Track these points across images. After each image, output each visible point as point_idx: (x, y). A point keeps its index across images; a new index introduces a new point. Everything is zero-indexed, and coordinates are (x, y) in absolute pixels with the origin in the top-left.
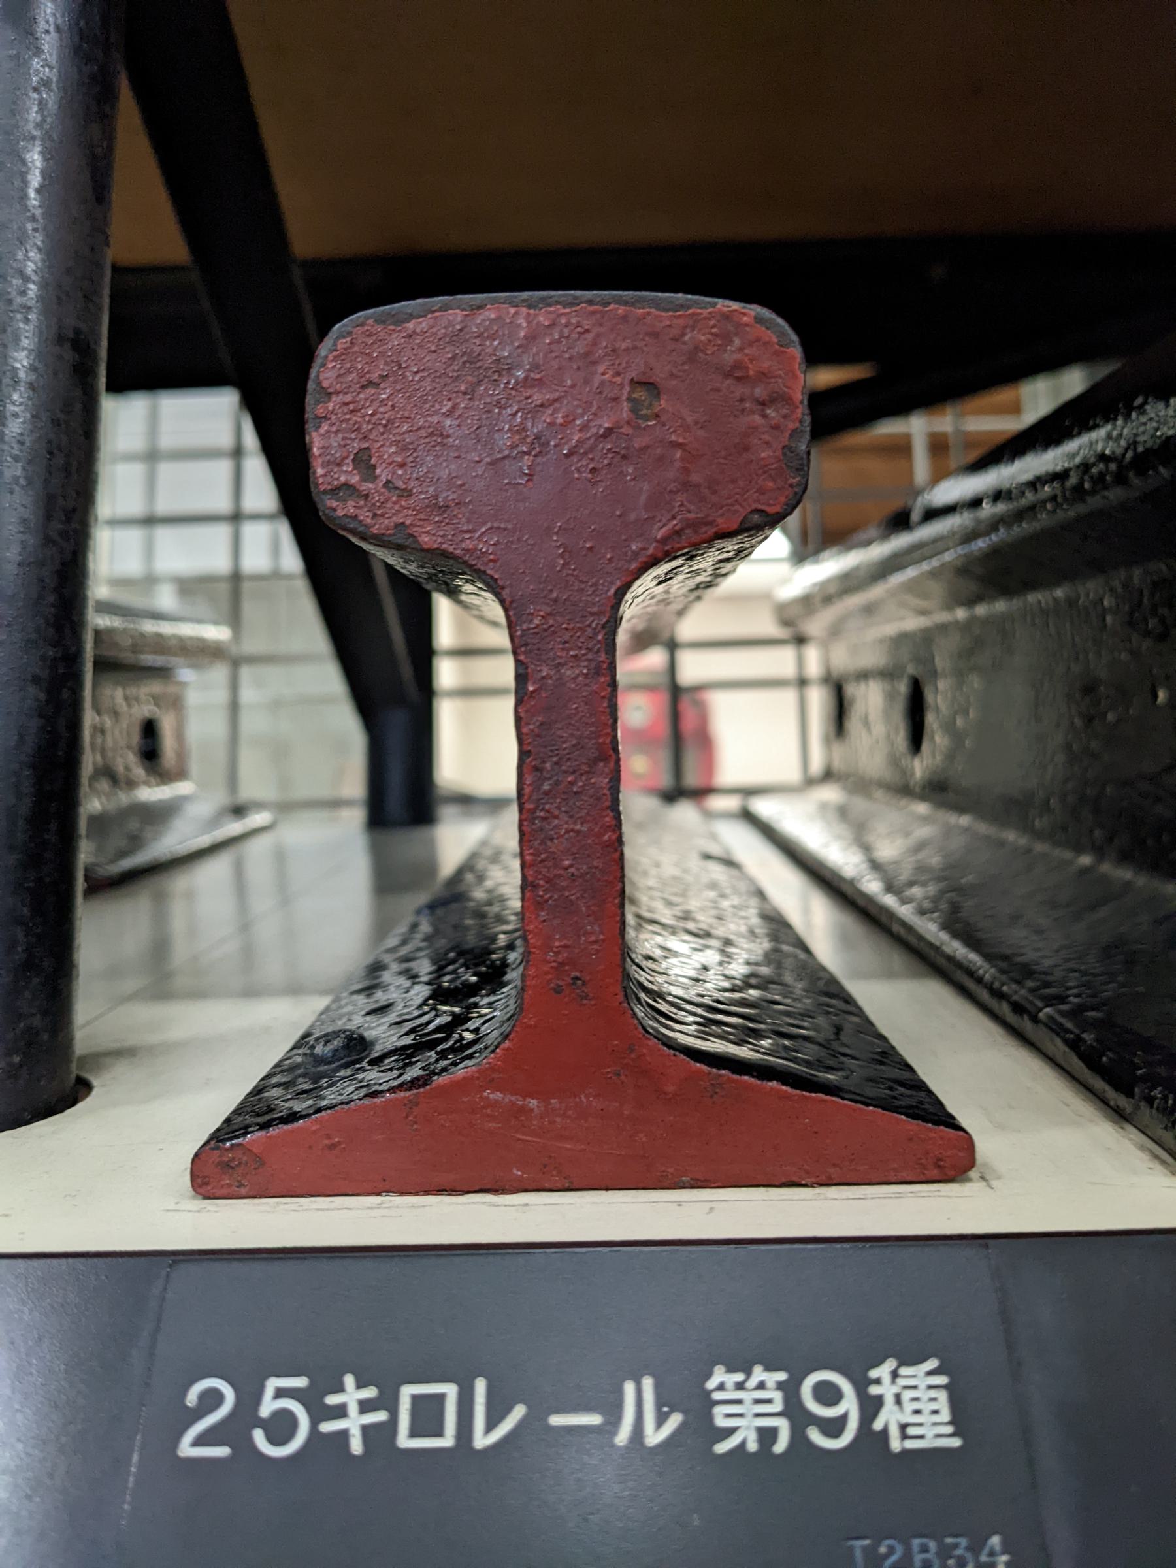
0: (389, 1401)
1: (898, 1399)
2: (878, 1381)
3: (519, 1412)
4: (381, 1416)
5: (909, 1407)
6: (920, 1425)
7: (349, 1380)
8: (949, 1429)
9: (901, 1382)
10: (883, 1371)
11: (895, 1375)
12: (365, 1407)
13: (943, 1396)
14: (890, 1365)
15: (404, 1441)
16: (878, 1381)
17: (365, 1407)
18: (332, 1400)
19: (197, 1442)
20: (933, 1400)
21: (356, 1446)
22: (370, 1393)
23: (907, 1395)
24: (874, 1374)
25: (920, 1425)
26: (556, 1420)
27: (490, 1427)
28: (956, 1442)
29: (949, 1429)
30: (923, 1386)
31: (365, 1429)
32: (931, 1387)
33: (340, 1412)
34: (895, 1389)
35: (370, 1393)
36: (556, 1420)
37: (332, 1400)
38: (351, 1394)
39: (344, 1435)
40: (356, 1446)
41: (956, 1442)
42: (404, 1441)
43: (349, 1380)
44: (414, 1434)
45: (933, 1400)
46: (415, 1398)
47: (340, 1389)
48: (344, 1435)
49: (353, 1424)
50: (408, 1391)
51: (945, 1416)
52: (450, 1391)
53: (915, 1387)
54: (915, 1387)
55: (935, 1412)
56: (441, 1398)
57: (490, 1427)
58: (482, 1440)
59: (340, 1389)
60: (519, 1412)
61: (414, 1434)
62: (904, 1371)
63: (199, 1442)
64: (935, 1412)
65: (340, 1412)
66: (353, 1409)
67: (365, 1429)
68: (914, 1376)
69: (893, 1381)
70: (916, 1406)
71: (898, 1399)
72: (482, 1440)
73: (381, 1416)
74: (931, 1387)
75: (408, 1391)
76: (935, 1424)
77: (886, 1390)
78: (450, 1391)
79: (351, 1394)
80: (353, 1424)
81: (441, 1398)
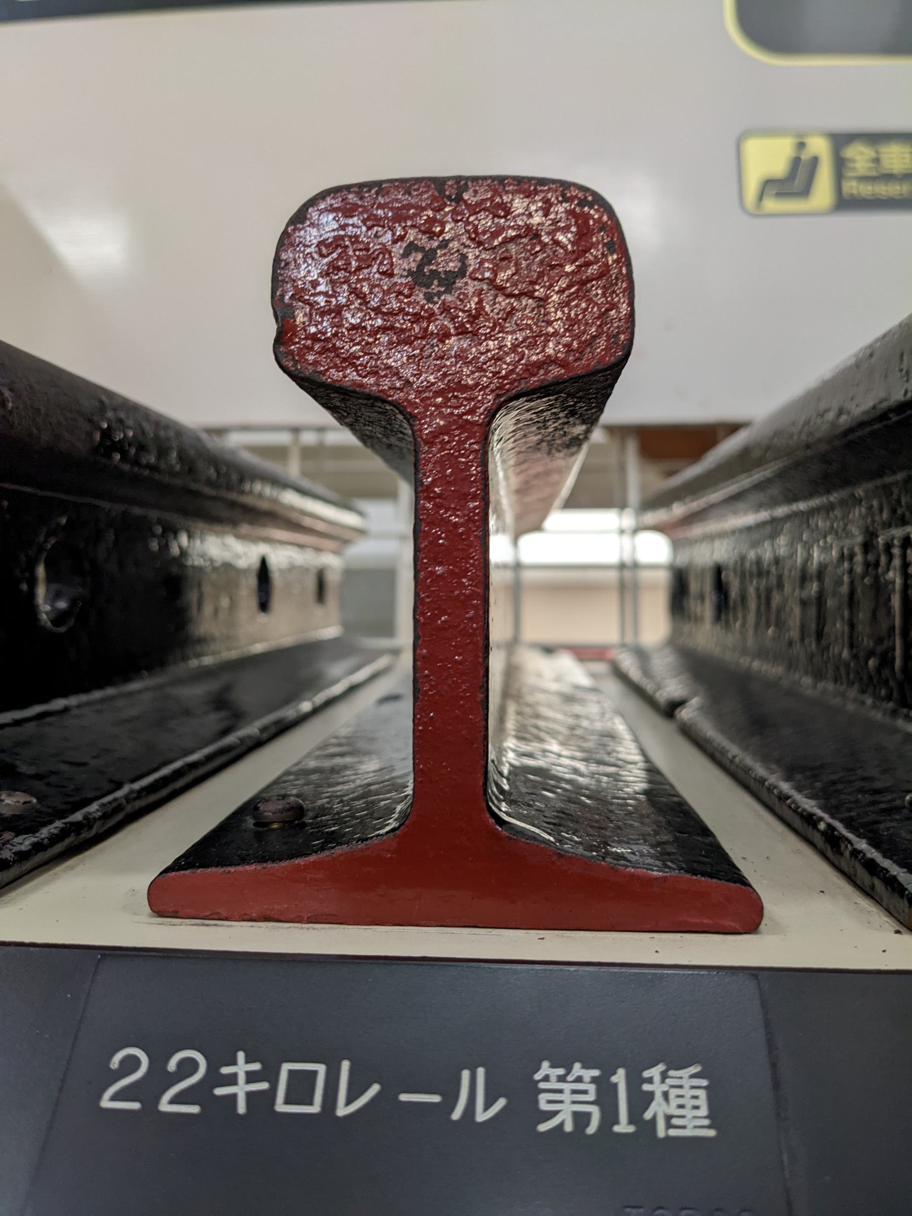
0: (270, 1074)
1: (666, 1095)
2: (650, 1081)
3: (375, 1089)
4: (264, 1086)
5: (674, 1102)
6: (683, 1117)
7: (241, 1056)
8: (706, 1122)
9: (669, 1081)
10: (655, 1072)
11: (664, 1076)
12: (251, 1077)
13: (702, 1094)
14: (661, 1067)
15: (281, 1107)
16: (650, 1081)
17: (251, 1077)
18: (225, 1070)
19: (114, 1098)
20: (696, 1097)
21: (242, 1108)
22: (256, 1066)
23: (673, 1093)
24: (646, 1074)
25: (683, 1117)
26: (404, 1097)
27: (349, 1102)
28: (712, 1133)
29: (706, 1122)
30: (687, 1086)
31: (250, 1095)
32: (693, 1087)
33: (232, 1080)
34: (665, 1088)
35: (256, 1066)
36: (404, 1097)
37: (225, 1070)
38: (242, 1067)
39: (234, 1097)
40: (242, 1108)
41: (712, 1133)
42: (281, 1107)
43: (241, 1056)
44: (287, 1102)
45: (696, 1097)
46: (291, 1073)
47: (234, 1063)
48: (234, 1097)
49: (241, 1090)
50: (286, 1067)
51: (704, 1111)
52: (321, 1069)
53: (681, 1087)
54: (681, 1087)
55: (696, 1108)
56: (314, 1073)
57: (349, 1102)
58: (342, 1111)
59: (234, 1063)
60: (375, 1089)
61: (287, 1102)
62: (672, 1073)
63: (114, 1098)
64: (696, 1108)
65: (232, 1080)
66: (242, 1078)
67: (250, 1095)
68: (681, 1078)
69: (663, 1081)
70: (680, 1101)
71: (666, 1095)
72: (342, 1111)
73: (264, 1086)
74: (693, 1087)
75: (286, 1067)
76: (695, 1117)
77: (657, 1088)
78: (321, 1069)
79: (242, 1067)
80: (241, 1090)
81: (314, 1073)
